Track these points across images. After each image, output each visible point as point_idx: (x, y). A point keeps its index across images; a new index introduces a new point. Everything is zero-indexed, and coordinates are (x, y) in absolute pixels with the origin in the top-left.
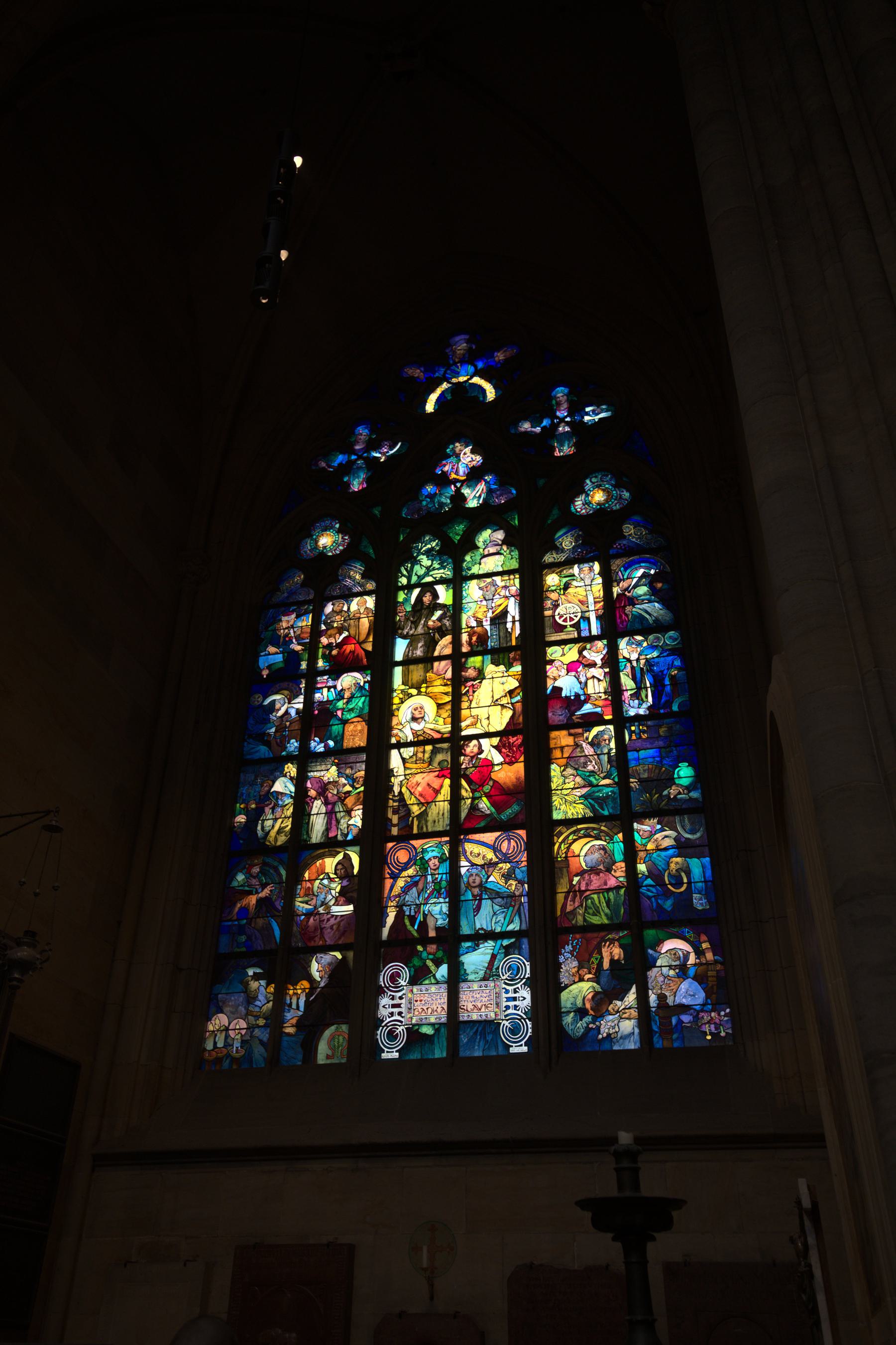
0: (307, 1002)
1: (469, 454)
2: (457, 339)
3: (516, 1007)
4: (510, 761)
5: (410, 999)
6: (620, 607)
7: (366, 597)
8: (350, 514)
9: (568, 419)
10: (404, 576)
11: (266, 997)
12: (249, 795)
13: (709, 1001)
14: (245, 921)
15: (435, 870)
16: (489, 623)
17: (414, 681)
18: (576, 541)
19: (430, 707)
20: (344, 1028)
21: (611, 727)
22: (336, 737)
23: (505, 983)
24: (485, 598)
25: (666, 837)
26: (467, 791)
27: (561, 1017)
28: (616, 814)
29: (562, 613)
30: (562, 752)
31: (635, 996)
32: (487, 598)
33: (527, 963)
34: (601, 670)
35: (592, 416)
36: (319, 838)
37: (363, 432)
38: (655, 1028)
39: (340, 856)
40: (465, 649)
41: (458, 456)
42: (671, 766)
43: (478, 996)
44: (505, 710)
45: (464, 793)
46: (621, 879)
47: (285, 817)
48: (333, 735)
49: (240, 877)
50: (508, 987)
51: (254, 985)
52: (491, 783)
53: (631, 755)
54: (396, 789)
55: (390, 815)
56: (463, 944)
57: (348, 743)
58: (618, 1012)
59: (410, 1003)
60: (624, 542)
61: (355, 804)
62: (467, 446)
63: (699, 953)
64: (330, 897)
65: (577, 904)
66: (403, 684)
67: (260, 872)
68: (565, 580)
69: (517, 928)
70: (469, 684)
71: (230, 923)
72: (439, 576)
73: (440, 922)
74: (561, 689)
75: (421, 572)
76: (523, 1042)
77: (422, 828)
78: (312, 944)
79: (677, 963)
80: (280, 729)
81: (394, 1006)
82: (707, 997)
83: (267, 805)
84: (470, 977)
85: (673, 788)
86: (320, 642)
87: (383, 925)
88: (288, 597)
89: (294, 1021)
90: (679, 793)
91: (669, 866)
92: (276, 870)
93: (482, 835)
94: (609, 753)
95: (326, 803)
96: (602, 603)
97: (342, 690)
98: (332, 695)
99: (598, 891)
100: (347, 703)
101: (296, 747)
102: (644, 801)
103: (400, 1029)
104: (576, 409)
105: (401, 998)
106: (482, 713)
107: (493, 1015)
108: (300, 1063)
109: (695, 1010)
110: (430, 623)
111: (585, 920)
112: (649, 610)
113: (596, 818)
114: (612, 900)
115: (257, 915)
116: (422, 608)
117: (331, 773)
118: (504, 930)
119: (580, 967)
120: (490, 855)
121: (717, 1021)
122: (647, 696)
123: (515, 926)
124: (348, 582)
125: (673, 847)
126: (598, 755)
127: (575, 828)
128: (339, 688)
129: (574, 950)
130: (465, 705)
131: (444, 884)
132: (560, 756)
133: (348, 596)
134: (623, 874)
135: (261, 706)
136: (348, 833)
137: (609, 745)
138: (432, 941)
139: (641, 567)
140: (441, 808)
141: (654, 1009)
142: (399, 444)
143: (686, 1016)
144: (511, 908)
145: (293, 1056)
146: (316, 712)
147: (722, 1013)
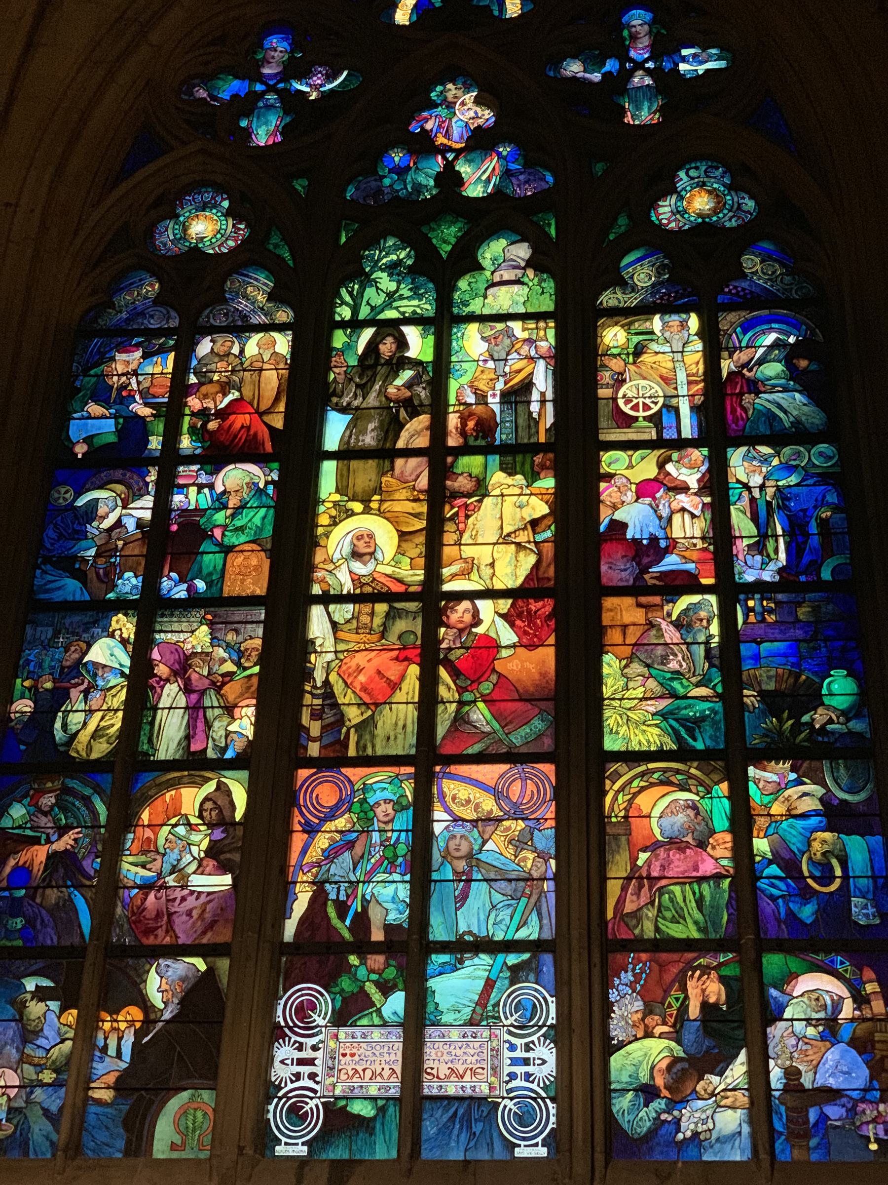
1: (470, 105)
3: (528, 1076)
4: (529, 644)
5: (333, 1051)
6: (732, 394)
7: (276, 335)
9: (650, 65)
10: (347, 304)
11: (59, 1033)
12: (41, 666)
13: (876, 1085)
14: (23, 892)
15: (386, 823)
16: (497, 399)
17: (359, 489)
18: (659, 274)
20: (207, 1096)
21: (713, 599)
22: (210, 574)
23: (510, 1033)
25: (805, 794)
26: (449, 689)
27: (610, 1099)
29: (630, 394)
30: (624, 634)
31: (744, 1068)
32: (496, 357)
34: (697, 499)
35: (693, 64)
36: (171, 751)
38: (778, 1126)
39: (211, 787)
40: (452, 442)
41: (450, 106)
42: (816, 673)
43: (459, 1052)
45: (443, 691)
46: (724, 862)
47: (108, 710)
49: (18, 812)
50: (514, 1040)
51: (35, 1009)
52: (494, 678)
53: (746, 650)
54: (319, 676)
55: (305, 720)
56: (433, 956)
57: (231, 588)
58: (713, 1095)
59: (333, 1058)
60: (745, 284)
61: (242, 694)
62: (467, 90)
63: (860, 1000)
65: (644, 900)
66: (338, 491)
67: (56, 804)
69: (534, 936)
70: (460, 501)
72: (411, 309)
73: (392, 917)
74: (624, 526)
76: (539, 1140)
77: (365, 747)
78: (151, 941)
79: (822, 1015)
81: (301, 1062)
82: (872, 1078)
83: (76, 685)
84: (446, 1018)
85: (820, 710)
86: (186, 404)
87: (284, 913)
89: (111, 1079)
90: (830, 721)
91: (809, 845)
92: (87, 801)
94: (707, 643)
95: (187, 690)
96: (701, 385)
97: (224, 492)
98: (205, 500)
100: (233, 516)
101: (135, 587)
102: (769, 730)
103: (312, 1104)
104: (665, 47)
105: (315, 1048)
106: (482, 554)
108: (120, 1155)
109: (851, 1098)
110: (391, 390)
111: (657, 929)
112: (785, 404)
113: (683, 754)
114: (708, 898)
115: (47, 883)
117: (198, 637)
118: (509, 937)
119: (648, 1011)
120: (489, 804)
122: (776, 551)
124: (243, 305)
125: (817, 813)
126: (688, 644)
128: (219, 488)
129: (637, 981)
130: (449, 538)
131: (402, 849)
132: (620, 640)
133: (242, 328)
134: (728, 854)
135: (71, 507)
137: (707, 628)
139: (772, 330)
141: (777, 1094)
142: (345, 73)
143: (836, 1108)
144: (524, 900)
146: (175, 528)
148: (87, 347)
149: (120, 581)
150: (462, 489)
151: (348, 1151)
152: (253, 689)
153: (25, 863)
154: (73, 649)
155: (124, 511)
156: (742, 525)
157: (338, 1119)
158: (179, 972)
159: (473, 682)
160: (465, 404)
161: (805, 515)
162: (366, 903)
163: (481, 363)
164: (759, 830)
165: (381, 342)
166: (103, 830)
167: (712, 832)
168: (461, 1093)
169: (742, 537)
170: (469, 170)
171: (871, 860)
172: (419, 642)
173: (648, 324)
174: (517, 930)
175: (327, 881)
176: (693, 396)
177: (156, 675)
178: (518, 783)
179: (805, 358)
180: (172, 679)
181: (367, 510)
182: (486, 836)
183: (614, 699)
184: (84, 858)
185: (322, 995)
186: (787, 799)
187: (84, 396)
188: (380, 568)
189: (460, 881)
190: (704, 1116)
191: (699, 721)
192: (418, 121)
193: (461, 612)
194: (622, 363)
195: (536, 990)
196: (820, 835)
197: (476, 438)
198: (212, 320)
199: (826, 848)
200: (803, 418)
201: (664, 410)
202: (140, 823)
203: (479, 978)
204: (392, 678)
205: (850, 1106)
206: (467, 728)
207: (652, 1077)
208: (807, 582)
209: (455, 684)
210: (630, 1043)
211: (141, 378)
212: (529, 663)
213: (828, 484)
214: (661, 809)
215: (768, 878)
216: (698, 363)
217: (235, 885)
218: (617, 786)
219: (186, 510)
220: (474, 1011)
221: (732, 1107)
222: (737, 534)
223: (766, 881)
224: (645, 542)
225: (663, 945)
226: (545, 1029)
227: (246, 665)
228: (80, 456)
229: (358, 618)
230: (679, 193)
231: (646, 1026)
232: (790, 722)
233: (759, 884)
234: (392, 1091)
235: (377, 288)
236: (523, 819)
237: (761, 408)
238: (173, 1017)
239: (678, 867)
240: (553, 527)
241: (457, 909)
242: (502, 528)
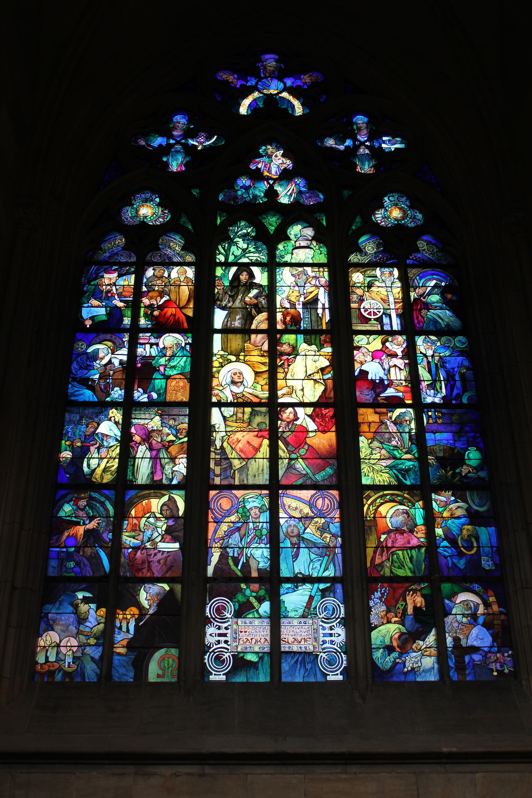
15: (256, 518)
19: (249, 375)
26: (284, 452)
36: (144, 480)
39: (165, 498)
40: (279, 326)
44: (317, 385)
45: (281, 453)
46: (422, 540)
47: (110, 458)
49: (67, 508)
52: (306, 447)
54: (218, 444)
55: (212, 465)
61: (179, 453)
66: (222, 350)
67: (87, 505)
70: (285, 357)
83: (93, 445)
91: (461, 532)
92: (103, 504)
93: (299, 491)
95: (151, 448)
113: (400, 487)
115: (85, 545)
120: (306, 510)
127: (381, 493)
130: (280, 376)
132: (367, 430)
134: (423, 536)
136: (173, 479)
140: (261, 465)
150: (286, 351)
152: (184, 449)
164: (438, 525)
167: (416, 525)
171: (490, 539)
172: (268, 428)
177: (134, 441)
180: (142, 443)
181: (238, 360)
182: (306, 526)
183: (366, 459)
186: (451, 510)
188: (246, 390)
191: (408, 471)
193: (288, 413)
196: (466, 527)
197: (291, 326)
199: (469, 533)
204: (255, 446)
209: (287, 449)
212: (324, 440)
215: (443, 547)
218: (369, 502)
223: (442, 549)
227: (180, 437)
229: (236, 415)
233: (438, 550)
236: (324, 518)
239: (400, 542)
240: (332, 372)
242: (306, 372)
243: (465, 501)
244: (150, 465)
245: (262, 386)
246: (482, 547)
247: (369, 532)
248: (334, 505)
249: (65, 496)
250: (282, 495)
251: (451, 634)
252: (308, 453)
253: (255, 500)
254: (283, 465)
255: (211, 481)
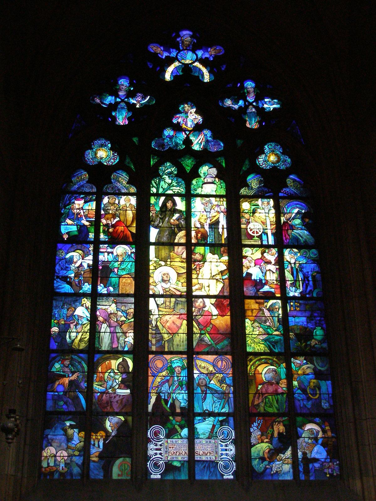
0: (104, 444)
1: (193, 114)
2: (185, 32)
3: (227, 454)
6: (285, 230)
8: (118, 139)
9: (254, 104)
13: (328, 457)
14: (62, 393)
16: (208, 226)
17: (163, 257)
18: (260, 184)
20: (128, 460)
21: (280, 301)
22: (114, 285)
23: (221, 441)
24: (205, 210)
25: (308, 367)
27: (251, 461)
28: (282, 351)
33: (232, 431)
37: (124, 83)
38: (301, 469)
39: (120, 360)
40: (193, 241)
41: (186, 113)
43: (206, 447)
44: (218, 283)
45: (194, 329)
46: (284, 389)
47: (84, 332)
48: (112, 284)
49: (57, 366)
51: (70, 431)
52: (211, 326)
54: (154, 323)
55: (150, 338)
58: (281, 460)
59: (167, 448)
60: (288, 190)
63: (324, 431)
64: (115, 384)
65: (260, 401)
66: (156, 257)
67: (70, 364)
68: (253, 207)
70: (197, 263)
71: (52, 393)
72: (176, 191)
73: (182, 405)
74: (251, 275)
75: (165, 186)
76: (231, 473)
77: (170, 348)
79: (313, 436)
80: (77, 275)
81: (157, 449)
82: (328, 454)
83: (72, 323)
84: (200, 437)
86: (101, 221)
87: (147, 403)
88: (78, 188)
89: (97, 454)
94: (278, 317)
95: (110, 326)
96: (275, 226)
98: (110, 258)
99: (272, 394)
101: (89, 289)
102: (298, 347)
103: (161, 462)
104: (259, 98)
105: (161, 445)
106: (205, 283)
107: (214, 458)
108: (102, 478)
110: (172, 221)
111: (265, 410)
113: (271, 353)
114: (280, 400)
116: (166, 211)
117: (112, 308)
119: (262, 435)
120: (211, 368)
121: (332, 467)
123: (226, 410)
124: (119, 185)
126: (272, 317)
127: (259, 358)
128: (115, 254)
130: (194, 276)
131: (184, 382)
133: (119, 194)
134: (285, 386)
136: (125, 346)
137: (278, 311)
138: (178, 414)
139: (297, 207)
140: (182, 337)
142: (149, 97)
144: (223, 400)
145: (97, 473)
146: (101, 268)
147: (335, 463)
148: (64, 198)
149: (83, 286)
150: (198, 259)
151: (173, 477)
153: (62, 383)
154: (70, 310)
155: (83, 261)
156: (289, 276)
157: (169, 467)
158: (116, 421)
159: (204, 327)
160: (197, 227)
161: (308, 274)
162: (174, 400)
163: (202, 213)
164: (295, 378)
165: (167, 202)
166: (86, 373)
168: (207, 459)
169: (289, 281)
170: (194, 139)
171: (328, 389)
173: (257, 202)
174: (222, 409)
175: (161, 392)
176: (272, 229)
177: (99, 321)
178: (220, 362)
179: (307, 218)
181: (166, 265)
182: (211, 379)
183: (249, 334)
184: (81, 382)
185: (162, 429)
186: (303, 369)
187: (65, 217)
188: (172, 286)
189: (204, 393)
190: (279, 466)
192: (176, 118)
193: (199, 303)
194: (249, 216)
195: (228, 428)
198: (107, 190)
200: (307, 240)
201: (263, 234)
202: (98, 371)
203: (211, 424)
204: (178, 324)
205: (321, 463)
206: (203, 343)
207: (264, 455)
208: (309, 297)
209: (199, 328)
210: (257, 444)
211: (84, 211)
212: (223, 321)
213: (315, 264)
214: (264, 371)
216: (273, 217)
217: (131, 393)
219: (104, 261)
220: (209, 434)
221: (287, 464)
222: (287, 280)
223: (297, 395)
224: (258, 281)
225: (265, 415)
226: (231, 440)
227: (129, 318)
228: (66, 239)
230: (265, 154)
231: (262, 439)
232: (304, 344)
234: (186, 459)
235: (165, 182)
236: (222, 374)
237: (293, 235)
238: (115, 435)
240: (228, 274)
241: (203, 402)
242: (211, 274)
243: (312, 363)
244: (110, 337)
245: (182, 283)
246: (323, 394)
247: (251, 384)
248: (229, 365)
249: (54, 358)
250: (195, 358)
251: (301, 450)
252: (212, 330)
253: (178, 361)
254: (196, 337)
255: (150, 349)
